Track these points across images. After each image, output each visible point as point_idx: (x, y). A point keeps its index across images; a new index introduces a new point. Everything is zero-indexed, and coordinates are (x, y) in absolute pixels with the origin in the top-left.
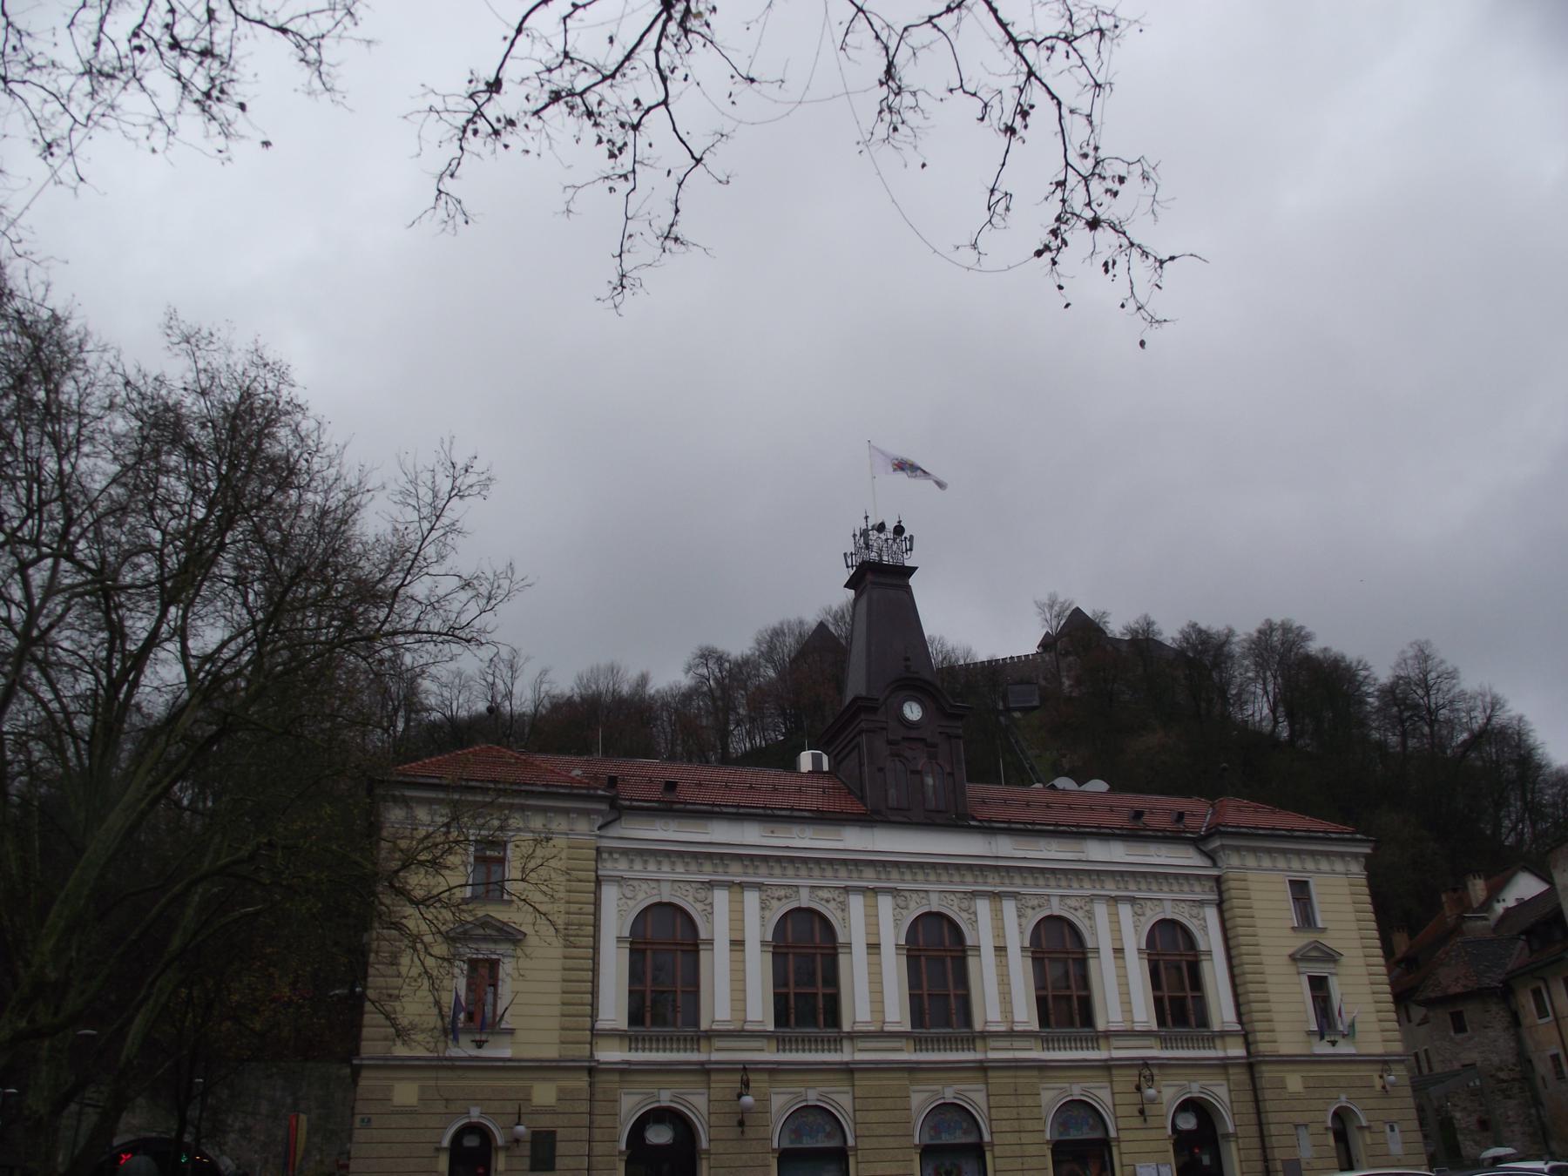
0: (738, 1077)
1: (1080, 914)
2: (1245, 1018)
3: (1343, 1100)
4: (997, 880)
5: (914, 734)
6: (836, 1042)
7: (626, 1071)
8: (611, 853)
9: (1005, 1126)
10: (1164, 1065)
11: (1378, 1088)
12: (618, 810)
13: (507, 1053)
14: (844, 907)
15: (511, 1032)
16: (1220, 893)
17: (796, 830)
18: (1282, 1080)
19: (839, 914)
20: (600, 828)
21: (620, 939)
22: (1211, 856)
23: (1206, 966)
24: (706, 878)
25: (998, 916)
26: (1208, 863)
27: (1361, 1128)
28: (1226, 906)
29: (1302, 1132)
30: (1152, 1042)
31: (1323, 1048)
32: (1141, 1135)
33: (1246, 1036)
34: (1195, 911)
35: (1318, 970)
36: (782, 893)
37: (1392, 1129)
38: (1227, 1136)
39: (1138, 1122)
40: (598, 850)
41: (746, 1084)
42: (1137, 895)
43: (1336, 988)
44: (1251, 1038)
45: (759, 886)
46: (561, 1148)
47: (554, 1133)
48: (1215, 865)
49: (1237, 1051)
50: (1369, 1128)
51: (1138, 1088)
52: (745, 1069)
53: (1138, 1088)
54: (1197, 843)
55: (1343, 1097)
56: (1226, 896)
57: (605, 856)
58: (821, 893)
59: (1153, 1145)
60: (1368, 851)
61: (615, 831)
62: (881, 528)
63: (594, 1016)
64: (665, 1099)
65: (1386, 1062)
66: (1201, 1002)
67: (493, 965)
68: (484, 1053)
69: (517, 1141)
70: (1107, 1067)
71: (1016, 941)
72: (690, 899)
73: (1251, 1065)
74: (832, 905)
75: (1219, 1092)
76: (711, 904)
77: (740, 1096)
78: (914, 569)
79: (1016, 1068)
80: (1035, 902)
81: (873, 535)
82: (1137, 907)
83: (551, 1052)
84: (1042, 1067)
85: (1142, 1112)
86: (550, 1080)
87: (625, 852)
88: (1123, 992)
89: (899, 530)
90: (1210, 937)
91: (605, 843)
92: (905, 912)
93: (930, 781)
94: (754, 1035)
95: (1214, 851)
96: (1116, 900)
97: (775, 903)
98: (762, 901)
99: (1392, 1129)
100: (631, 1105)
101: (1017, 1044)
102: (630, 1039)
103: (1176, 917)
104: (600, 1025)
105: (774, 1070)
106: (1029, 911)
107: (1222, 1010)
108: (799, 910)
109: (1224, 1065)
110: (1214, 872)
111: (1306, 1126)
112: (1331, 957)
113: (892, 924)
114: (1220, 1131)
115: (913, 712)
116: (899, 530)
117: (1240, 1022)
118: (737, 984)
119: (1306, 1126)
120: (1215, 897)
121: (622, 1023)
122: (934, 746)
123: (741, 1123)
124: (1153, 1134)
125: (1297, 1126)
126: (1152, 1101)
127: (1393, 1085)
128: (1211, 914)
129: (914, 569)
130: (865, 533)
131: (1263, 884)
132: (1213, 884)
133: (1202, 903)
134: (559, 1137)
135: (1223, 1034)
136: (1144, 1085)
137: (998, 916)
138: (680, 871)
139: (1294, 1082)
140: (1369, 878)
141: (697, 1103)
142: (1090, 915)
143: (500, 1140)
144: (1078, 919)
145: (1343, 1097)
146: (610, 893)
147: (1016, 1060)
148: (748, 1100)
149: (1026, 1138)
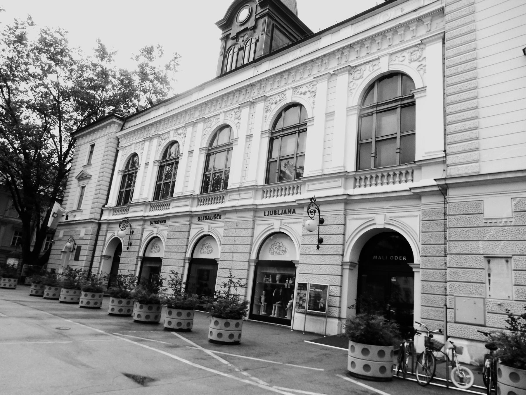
1: (308, 94)
4: (256, 92)
5: (243, 28)
7: (109, 223)
9: (227, 248)
21: (119, 172)
25: (252, 115)
29: (497, 266)
30: (340, 182)
32: (316, 259)
36: (166, 136)
39: (313, 249)
46: (82, 253)
47: (81, 247)
59: (325, 269)
67: (85, 187)
73: (443, 190)
79: (236, 211)
82: (357, 75)
84: (255, 210)
85: (320, 241)
86: (84, 227)
87: (125, 135)
90: (426, 72)
101: (243, 196)
102: (113, 210)
103: (393, 68)
104: (106, 206)
105: (144, 219)
109: (417, 195)
111: (507, 259)
119: (507, 259)
124: (327, 259)
125: (489, 259)
133: (422, 43)
134: (82, 248)
139: (498, 205)
142: (314, 94)
146: (120, 153)
149: (236, 257)
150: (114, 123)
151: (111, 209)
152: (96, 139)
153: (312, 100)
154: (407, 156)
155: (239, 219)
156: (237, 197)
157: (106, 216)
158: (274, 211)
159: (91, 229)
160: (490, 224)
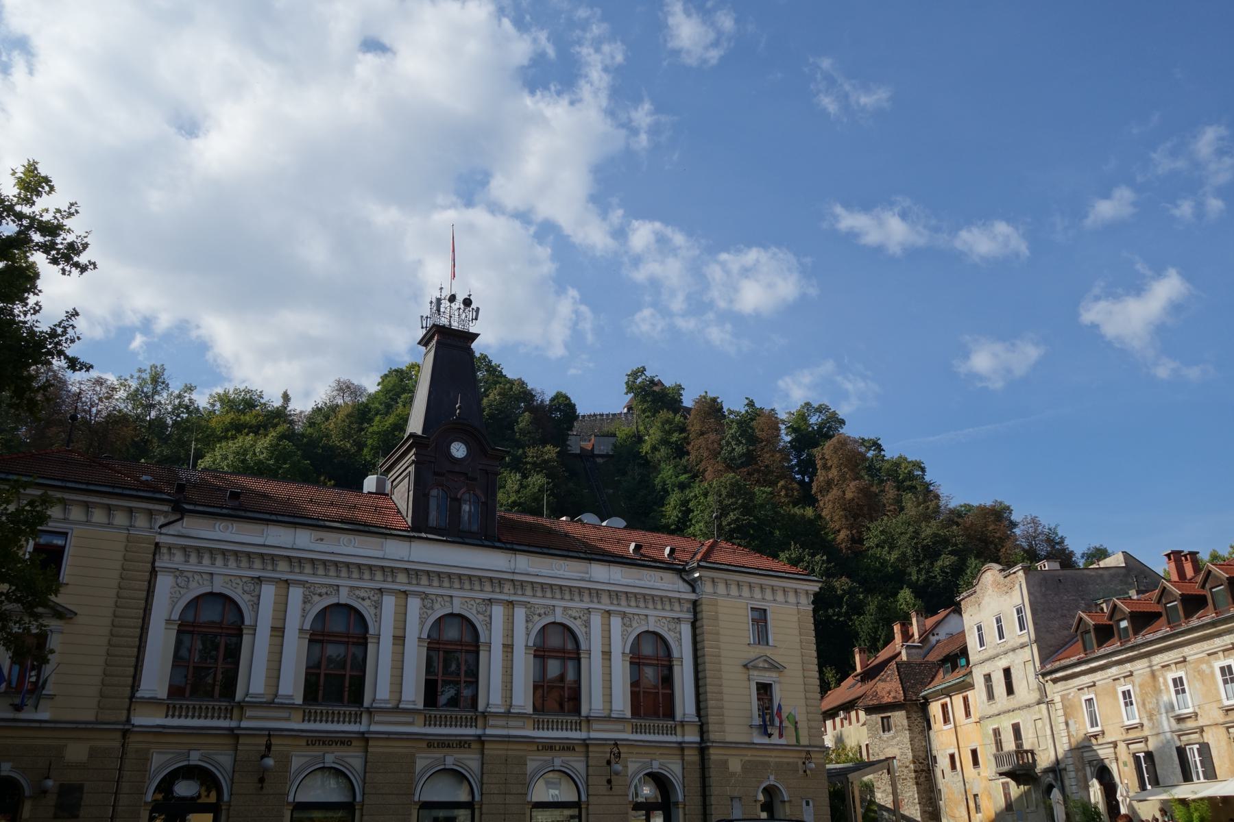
0: (264, 741)
1: (578, 622)
2: (702, 712)
3: (772, 780)
6: (357, 719)
7: (159, 732)
8: (170, 549)
10: (631, 744)
11: (801, 772)
12: (180, 510)
13: (45, 716)
14: (378, 605)
15: (51, 697)
16: (695, 613)
17: (345, 538)
18: (726, 762)
19: (372, 611)
20: (161, 527)
21: (169, 621)
22: (692, 585)
23: (676, 669)
24: (257, 574)
25: (510, 621)
26: (689, 588)
27: (784, 802)
28: (698, 624)
31: (759, 739)
33: (701, 727)
34: (672, 626)
35: (766, 677)
36: (324, 590)
37: (808, 804)
38: (677, 803)
39: (603, 789)
40: (157, 544)
41: (269, 747)
42: (628, 610)
43: (777, 694)
44: (705, 728)
45: (302, 583)
47: (80, 788)
48: (694, 591)
49: (692, 737)
50: (790, 801)
51: (609, 763)
52: (270, 734)
53: (609, 763)
54: (682, 572)
55: (772, 778)
56: (699, 616)
57: (164, 550)
58: (357, 592)
60: (817, 589)
61: (171, 530)
62: (452, 298)
63: (135, 686)
64: (195, 758)
65: (808, 752)
66: (670, 698)
68: (21, 715)
69: (45, 792)
70: (585, 744)
71: (521, 641)
72: (240, 591)
74: (367, 603)
75: (674, 768)
76: (259, 596)
77: (263, 757)
78: (477, 335)
80: (542, 611)
81: (445, 303)
83: (89, 716)
85: (609, 782)
87: (184, 549)
88: (607, 686)
89: (467, 302)
91: (159, 539)
92: (430, 612)
93: (466, 507)
94: (282, 706)
95: (695, 580)
96: (609, 612)
97: (316, 598)
98: (305, 596)
99: (808, 804)
100: (161, 762)
101: (511, 723)
104: (138, 695)
106: (536, 618)
107: (685, 704)
108: (338, 605)
109: (681, 747)
110: (693, 597)
111: (740, 798)
112: (774, 667)
113: (417, 621)
114: (673, 800)
115: (458, 450)
116: (467, 302)
117: (698, 714)
118: (274, 664)
120: (690, 616)
121: (162, 693)
122: (475, 479)
123: (262, 780)
126: (617, 774)
127: (811, 770)
128: (686, 629)
129: (477, 335)
130: (439, 301)
131: (729, 604)
132: (690, 606)
135: (682, 724)
136: (613, 761)
137: (510, 621)
138: (232, 568)
140: (814, 610)
141: (222, 761)
142: (587, 624)
143: (27, 793)
144: (577, 626)
145: (772, 778)
146: (164, 584)
147: (509, 736)
148: (270, 762)
150: (165, 513)
151: (153, 702)
152: (65, 520)
153: (583, 629)
154: (670, 714)
155: (510, 753)
156: (502, 722)
157: (142, 719)
158: (549, 747)
159: (114, 743)
160: (733, 774)
